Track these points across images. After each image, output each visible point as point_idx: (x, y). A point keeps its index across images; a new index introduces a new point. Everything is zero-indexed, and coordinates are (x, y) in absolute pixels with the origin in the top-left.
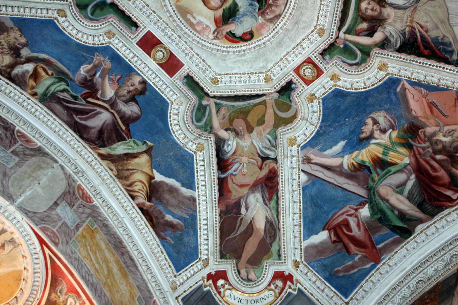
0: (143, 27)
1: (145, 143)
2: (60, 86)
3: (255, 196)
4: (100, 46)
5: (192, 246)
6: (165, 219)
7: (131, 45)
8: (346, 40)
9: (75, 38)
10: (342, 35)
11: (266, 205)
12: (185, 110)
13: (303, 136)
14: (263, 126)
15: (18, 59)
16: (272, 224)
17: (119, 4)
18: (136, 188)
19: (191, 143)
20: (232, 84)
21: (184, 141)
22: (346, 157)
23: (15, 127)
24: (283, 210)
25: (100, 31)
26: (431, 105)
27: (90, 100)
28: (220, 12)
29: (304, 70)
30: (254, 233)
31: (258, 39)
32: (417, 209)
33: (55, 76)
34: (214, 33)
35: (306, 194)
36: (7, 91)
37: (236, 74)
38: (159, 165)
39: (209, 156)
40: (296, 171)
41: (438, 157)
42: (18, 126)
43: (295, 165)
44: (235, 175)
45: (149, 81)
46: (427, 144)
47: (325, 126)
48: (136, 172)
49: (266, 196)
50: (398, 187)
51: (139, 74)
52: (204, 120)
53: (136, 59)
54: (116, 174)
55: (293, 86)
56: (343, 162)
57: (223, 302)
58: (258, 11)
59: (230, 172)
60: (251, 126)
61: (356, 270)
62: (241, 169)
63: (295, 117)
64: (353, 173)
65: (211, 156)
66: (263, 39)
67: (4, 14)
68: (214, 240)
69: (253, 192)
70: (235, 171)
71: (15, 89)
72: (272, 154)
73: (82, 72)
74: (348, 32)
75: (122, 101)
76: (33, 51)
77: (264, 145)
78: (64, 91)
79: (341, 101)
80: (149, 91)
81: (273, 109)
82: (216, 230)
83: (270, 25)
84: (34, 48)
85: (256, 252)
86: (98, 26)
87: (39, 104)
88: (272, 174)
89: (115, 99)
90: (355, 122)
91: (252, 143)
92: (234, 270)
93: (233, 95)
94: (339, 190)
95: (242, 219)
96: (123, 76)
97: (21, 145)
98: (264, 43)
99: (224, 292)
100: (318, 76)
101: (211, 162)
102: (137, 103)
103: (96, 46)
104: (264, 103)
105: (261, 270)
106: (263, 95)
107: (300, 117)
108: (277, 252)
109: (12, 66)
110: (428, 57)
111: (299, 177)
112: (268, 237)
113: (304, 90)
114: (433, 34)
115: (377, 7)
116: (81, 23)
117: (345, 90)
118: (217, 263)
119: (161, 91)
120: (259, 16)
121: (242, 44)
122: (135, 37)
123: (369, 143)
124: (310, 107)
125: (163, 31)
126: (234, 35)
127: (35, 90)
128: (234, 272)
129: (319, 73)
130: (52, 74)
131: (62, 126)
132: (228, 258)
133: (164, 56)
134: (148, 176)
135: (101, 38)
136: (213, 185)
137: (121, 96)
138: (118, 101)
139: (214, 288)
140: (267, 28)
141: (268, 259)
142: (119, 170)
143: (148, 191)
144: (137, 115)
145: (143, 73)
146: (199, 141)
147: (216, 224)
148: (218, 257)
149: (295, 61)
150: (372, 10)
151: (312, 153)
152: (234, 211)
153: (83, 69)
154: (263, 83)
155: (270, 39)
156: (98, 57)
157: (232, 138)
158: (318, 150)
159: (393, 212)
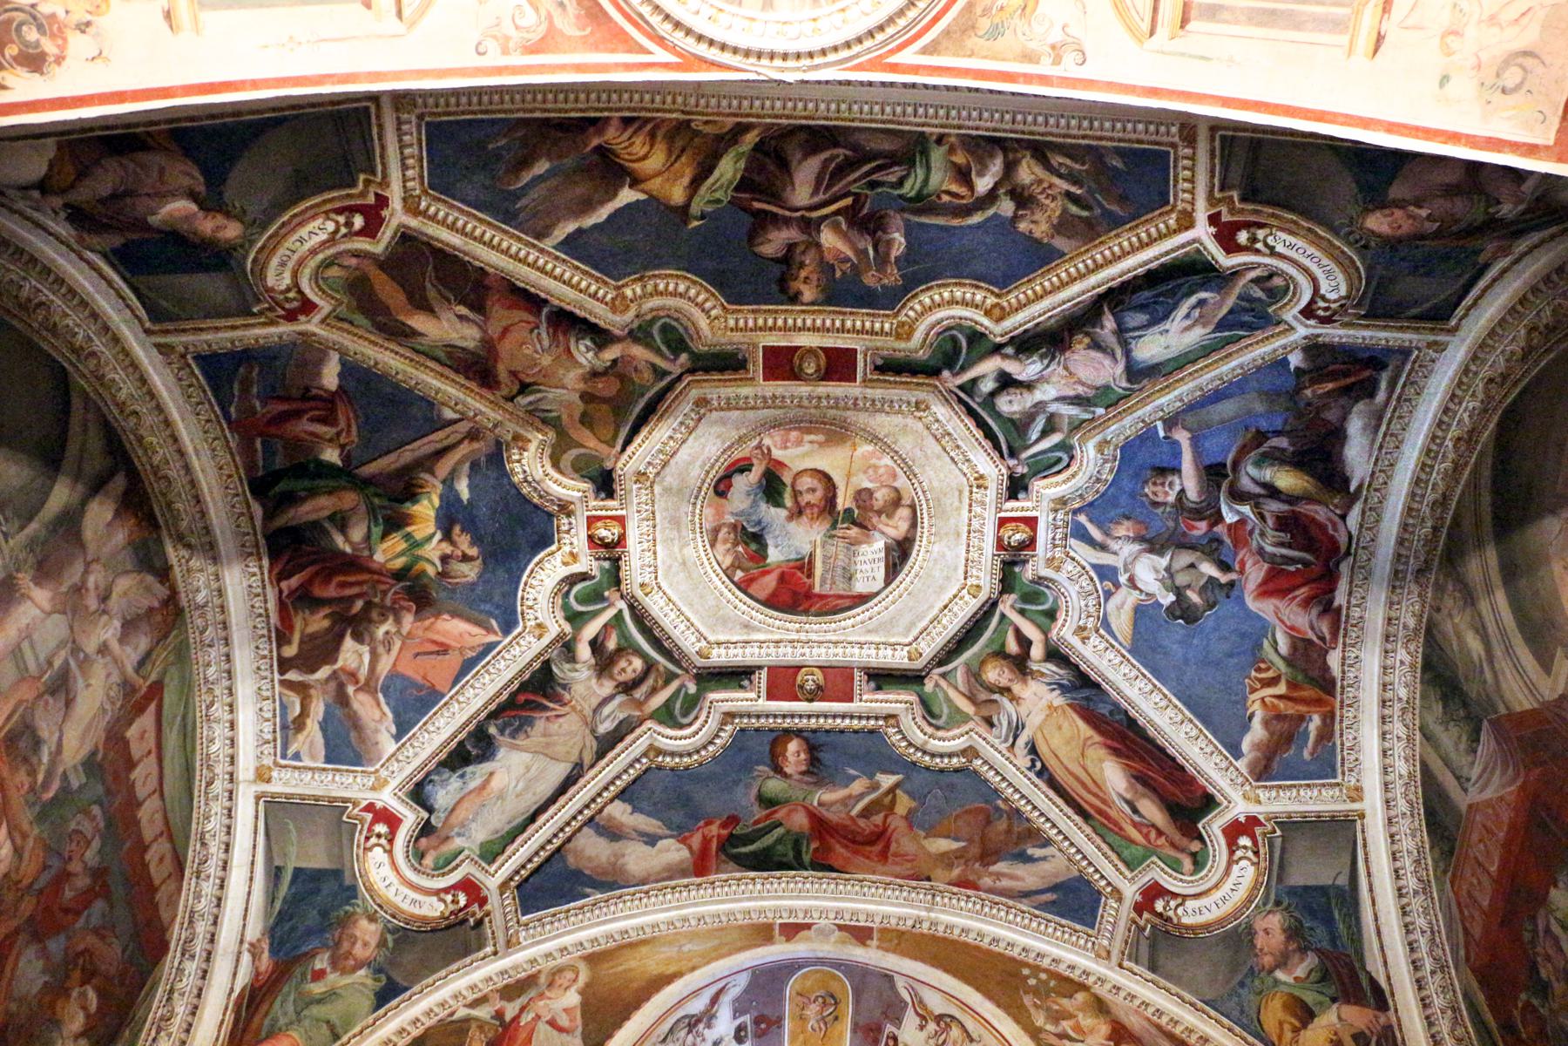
1: (702, 217)
8: (611, 605)
10: (622, 605)
18: (638, 140)
26: (443, 649)
27: (849, 201)
28: (787, 478)
41: (359, 604)
44: (532, 331)
46: (388, 602)
50: (343, 518)
51: (813, 304)
59: (544, 326)
69: (482, 340)
72: (523, 400)
73: (896, 235)
74: (619, 616)
78: (900, 183)
91: (563, 387)
95: (449, 301)
100: (590, 538)
102: (776, 260)
106: (624, 449)
109: (1010, 168)
110: (513, 695)
114: (540, 725)
115: (622, 678)
117: (542, 554)
121: (721, 472)
123: (438, 528)
126: (742, 471)
127: (944, 148)
130: (939, 197)
138: (804, 237)
150: (623, 670)
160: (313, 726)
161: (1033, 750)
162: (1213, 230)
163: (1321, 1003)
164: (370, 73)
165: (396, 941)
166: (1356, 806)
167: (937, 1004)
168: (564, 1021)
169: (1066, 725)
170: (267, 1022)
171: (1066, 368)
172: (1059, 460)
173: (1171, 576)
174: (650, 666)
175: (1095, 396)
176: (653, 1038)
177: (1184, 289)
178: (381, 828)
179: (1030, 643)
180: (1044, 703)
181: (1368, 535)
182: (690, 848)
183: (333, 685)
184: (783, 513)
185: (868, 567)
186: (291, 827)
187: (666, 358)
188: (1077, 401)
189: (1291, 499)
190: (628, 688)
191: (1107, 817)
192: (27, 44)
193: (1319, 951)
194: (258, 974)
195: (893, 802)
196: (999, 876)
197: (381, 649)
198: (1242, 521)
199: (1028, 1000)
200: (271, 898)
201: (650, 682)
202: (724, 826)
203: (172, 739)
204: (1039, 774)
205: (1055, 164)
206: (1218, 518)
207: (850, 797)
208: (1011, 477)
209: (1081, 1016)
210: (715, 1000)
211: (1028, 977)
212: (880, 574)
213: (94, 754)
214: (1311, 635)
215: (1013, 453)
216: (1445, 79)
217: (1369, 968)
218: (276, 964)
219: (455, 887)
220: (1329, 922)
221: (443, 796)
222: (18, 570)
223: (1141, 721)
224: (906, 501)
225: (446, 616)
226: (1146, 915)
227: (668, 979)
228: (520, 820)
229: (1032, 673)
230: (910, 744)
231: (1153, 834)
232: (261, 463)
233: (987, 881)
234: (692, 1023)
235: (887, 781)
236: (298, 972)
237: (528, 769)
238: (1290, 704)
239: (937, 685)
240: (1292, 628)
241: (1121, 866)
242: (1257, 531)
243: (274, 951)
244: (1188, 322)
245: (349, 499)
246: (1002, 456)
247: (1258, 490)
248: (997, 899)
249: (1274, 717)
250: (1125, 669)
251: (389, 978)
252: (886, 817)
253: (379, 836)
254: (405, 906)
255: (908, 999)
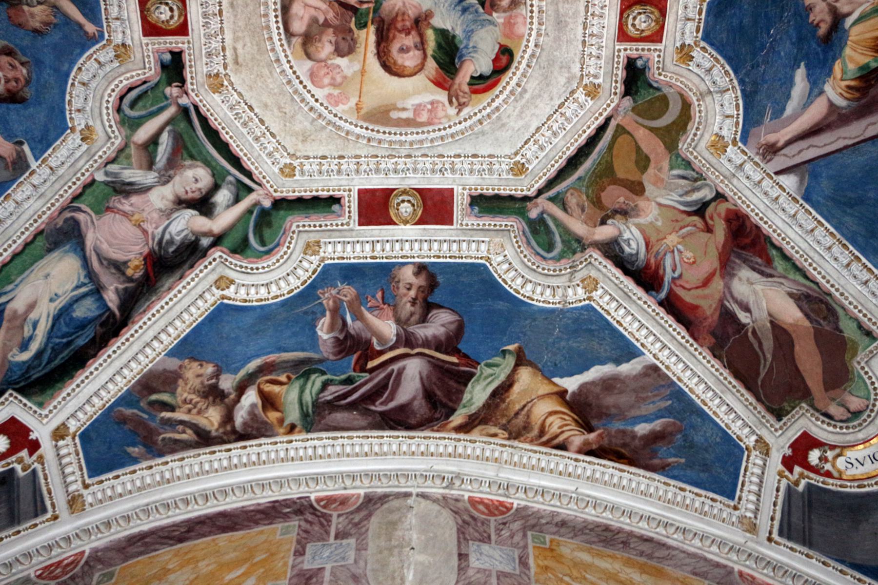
0: (346, 194)
1: (504, 352)
2: (313, 383)
3: (740, 279)
4: (314, 277)
5: (718, 440)
6: (639, 435)
7: (354, 233)
9: (272, 299)
11: (771, 276)
12: (517, 252)
13: (728, 121)
14: (652, 165)
15: (226, 400)
16: (807, 297)
17: (284, 194)
18: (554, 429)
19: (570, 292)
20: (548, 149)
21: (557, 297)
22: (828, 88)
23: (308, 497)
24: (806, 260)
25: (294, 257)
27: (371, 364)
28: (431, 65)
29: (633, 25)
30: (794, 336)
31: (523, 48)
33: (294, 377)
34: (451, 102)
35: (818, 202)
36: (254, 458)
37: (538, 129)
38: (556, 365)
39: (616, 285)
40: (767, 183)
42: (311, 493)
43: (757, 177)
44: (680, 276)
45: (426, 260)
47: (747, 74)
48: (532, 407)
49: (757, 263)
52: (557, 238)
53: (378, 247)
54: (507, 435)
55: (639, 63)
56: (829, 100)
57: (849, 484)
58: (483, 8)
59: (667, 278)
60: (633, 182)
62: (681, 259)
63: (686, 106)
64: (864, 101)
65: (617, 282)
66: (528, 41)
67: (155, 358)
68: (741, 402)
70: (674, 271)
71: (261, 445)
72: (706, 194)
73: (325, 337)
75: (417, 324)
76: (236, 371)
77: (680, 191)
78: (325, 385)
79: (735, 14)
80: (441, 273)
81: (644, 126)
82: (730, 383)
83: (519, 11)
84: (233, 366)
85: (825, 363)
86: (285, 253)
87: (310, 436)
88: (734, 222)
89: (405, 330)
90: (789, 22)
91: (660, 205)
92: (817, 419)
93: (564, 163)
94: (868, 147)
95: (754, 332)
96: (385, 287)
97: (339, 516)
98: (536, 46)
99: (834, 466)
101: (626, 290)
102: (439, 307)
103: (309, 282)
104: (621, 130)
105: (861, 383)
106: (608, 120)
107: (694, 99)
108: (859, 332)
109: (228, 418)
111: (781, 187)
112: (822, 321)
113: (662, 54)
116: (261, 271)
118: (780, 432)
119: (455, 257)
120: (491, 15)
121: (505, 78)
122: (350, 217)
123: (846, 32)
124: (696, 70)
125: (377, 171)
126: (481, 77)
127: (287, 422)
128: (819, 423)
130: (289, 378)
131: (368, 437)
132: (789, 409)
133: (413, 205)
134: (554, 397)
135: (305, 264)
136: (662, 322)
137: (408, 319)
138: (411, 329)
139: (812, 475)
140: (520, 20)
141: (855, 354)
142: (504, 425)
143: (576, 417)
144: (456, 324)
145: (408, 257)
146: (579, 276)
147: (721, 374)
148: (772, 422)
149: (606, 25)
151: (765, 134)
152: (730, 330)
153: (322, 330)
154: (591, 103)
155: (539, 30)
156: (326, 295)
158: (771, 119)
162: (33, 436)
171: (145, 232)
172: (132, 105)
175: (107, 198)
177: (46, 357)
184: (438, 22)
187: (550, 215)
188: (125, 189)
205: (189, 431)
208: (183, 81)
215: (185, 111)
224: (297, 41)
244: (33, 316)
246: (196, 108)
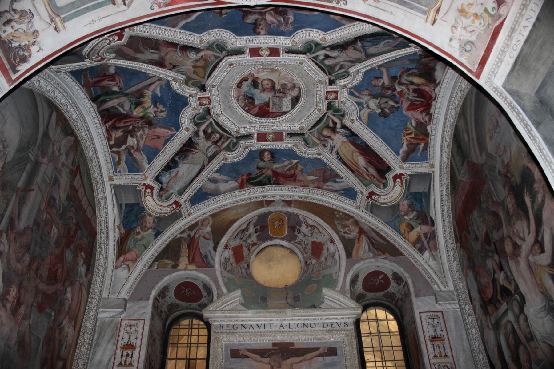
8: (208, 120)
10: (211, 120)
22: (151, 93)
26: (159, 137)
28: (260, 82)
32: (106, 108)
34: (253, 74)
41: (131, 127)
44: (175, 52)
47: (173, 93)
50: (122, 105)
61: (83, 77)
69: (159, 57)
73: (291, 16)
74: (211, 123)
91: (187, 65)
95: (147, 49)
102: (251, 24)
110: (181, 148)
114: (191, 156)
115: (214, 140)
126: (245, 81)
129: (201, 104)
138: (260, 17)
150: (214, 138)
157: (196, 57)
159: (109, 98)
160: (123, 163)
161: (338, 153)
163: (416, 225)
164: (119, 23)
165: (158, 221)
166: (432, 169)
167: (310, 222)
168: (207, 236)
169: (347, 147)
170: (127, 247)
172: (345, 75)
173: (380, 105)
174: (222, 136)
176: (232, 238)
178: (148, 190)
179: (336, 124)
180: (341, 140)
181: (441, 95)
182: (238, 182)
183: (127, 151)
184: (259, 91)
185: (286, 104)
186: (122, 192)
189: (418, 85)
190: (215, 143)
191: (359, 172)
192: (21, 56)
193: (417, 211)
194: (121, 234)
195: (297, 167)
196: (328, 186)
197: (140, 139)
198: (402, 91)
199: (336, 222)
200: (120, 213)
201: (222, 140)
202: (248, 175)
203: (85, 178)
204: (339, 160)
206: (395, 90)
207: (284, 166)
209: (351, 226)
210: (248, 224)
211: (336, 214)
212: (290, 106)
213: (68, 195)
214: (422, 121)
215: (330, 74)
216: (451, 40)
217: (430, 215)
218: (126, 231)
219: (172, 204)
220: (421, 202)
221: (165, 179)
222: (38, 157)
223: (370, 145)
224: (297, 86)
225: (158, 128)
226: (370, 199)
227: (235, 221)
228: (188, 182)
229: (337, 132)
230: (301, 152)
231: (372, 178)
232: (93, 93)
233: (325, 187)
234: (243, 231)
235: (295, 161)
236: (133, 233)
237: (189, 168)
238: (415, 140)
239: (309, 135)
240: (417, 119)
241: (363, 186)
242: (407, 93)
243: (125, 227)
245: (123, 99)
247: (407, 82)
248: (328, 192)
249: (410, 144)
250: (365, 130)
251: (157, 230)
252: (295, 171)
253: (148, 193)
254: (159, 211)
255: (303, 221)
